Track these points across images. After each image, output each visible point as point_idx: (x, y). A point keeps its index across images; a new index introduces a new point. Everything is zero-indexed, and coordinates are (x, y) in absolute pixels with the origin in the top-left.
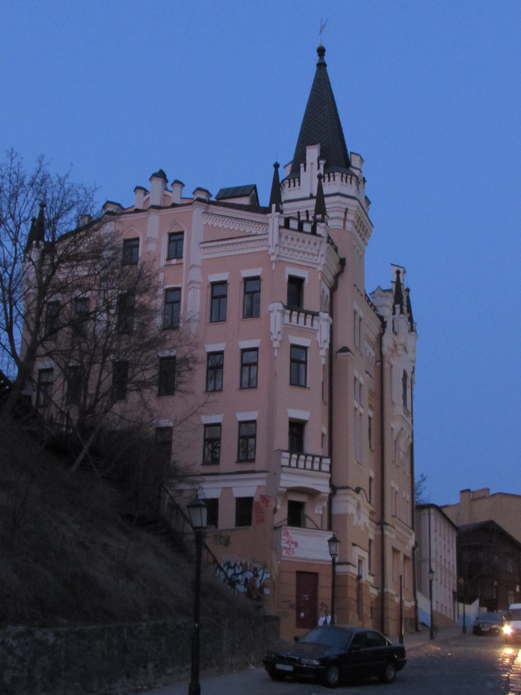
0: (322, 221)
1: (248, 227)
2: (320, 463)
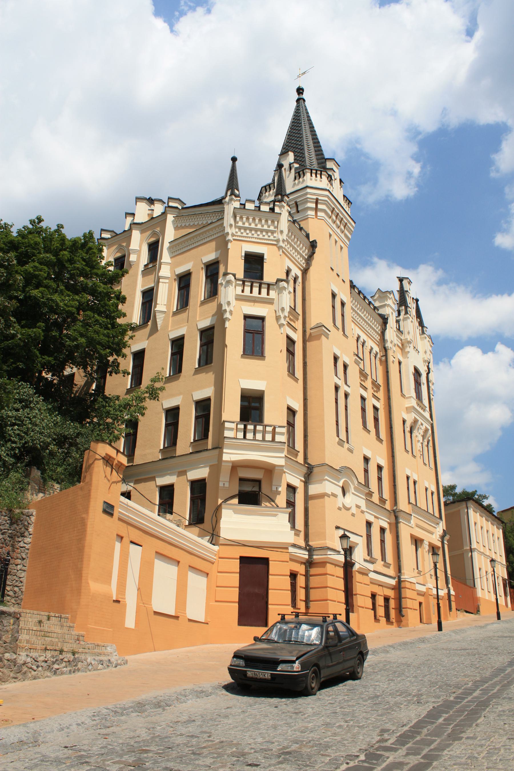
1: (209, 218)
2: (274, 433)
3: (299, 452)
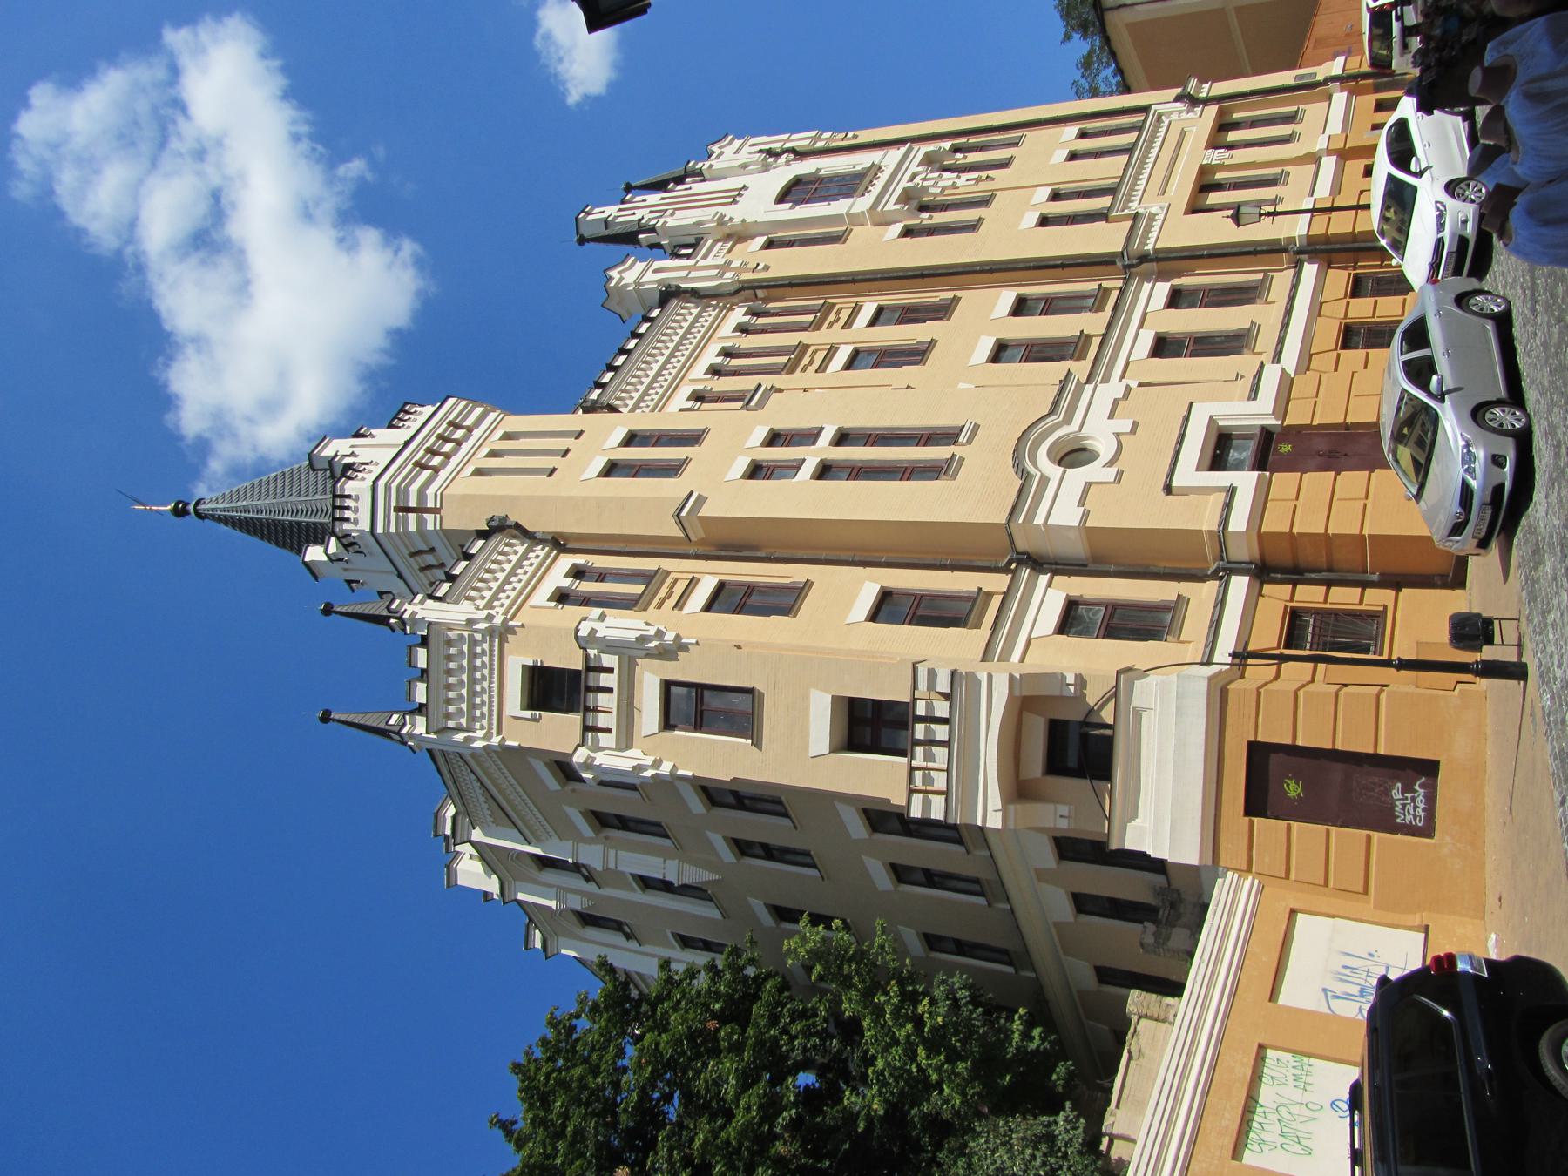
3: (980, 589)
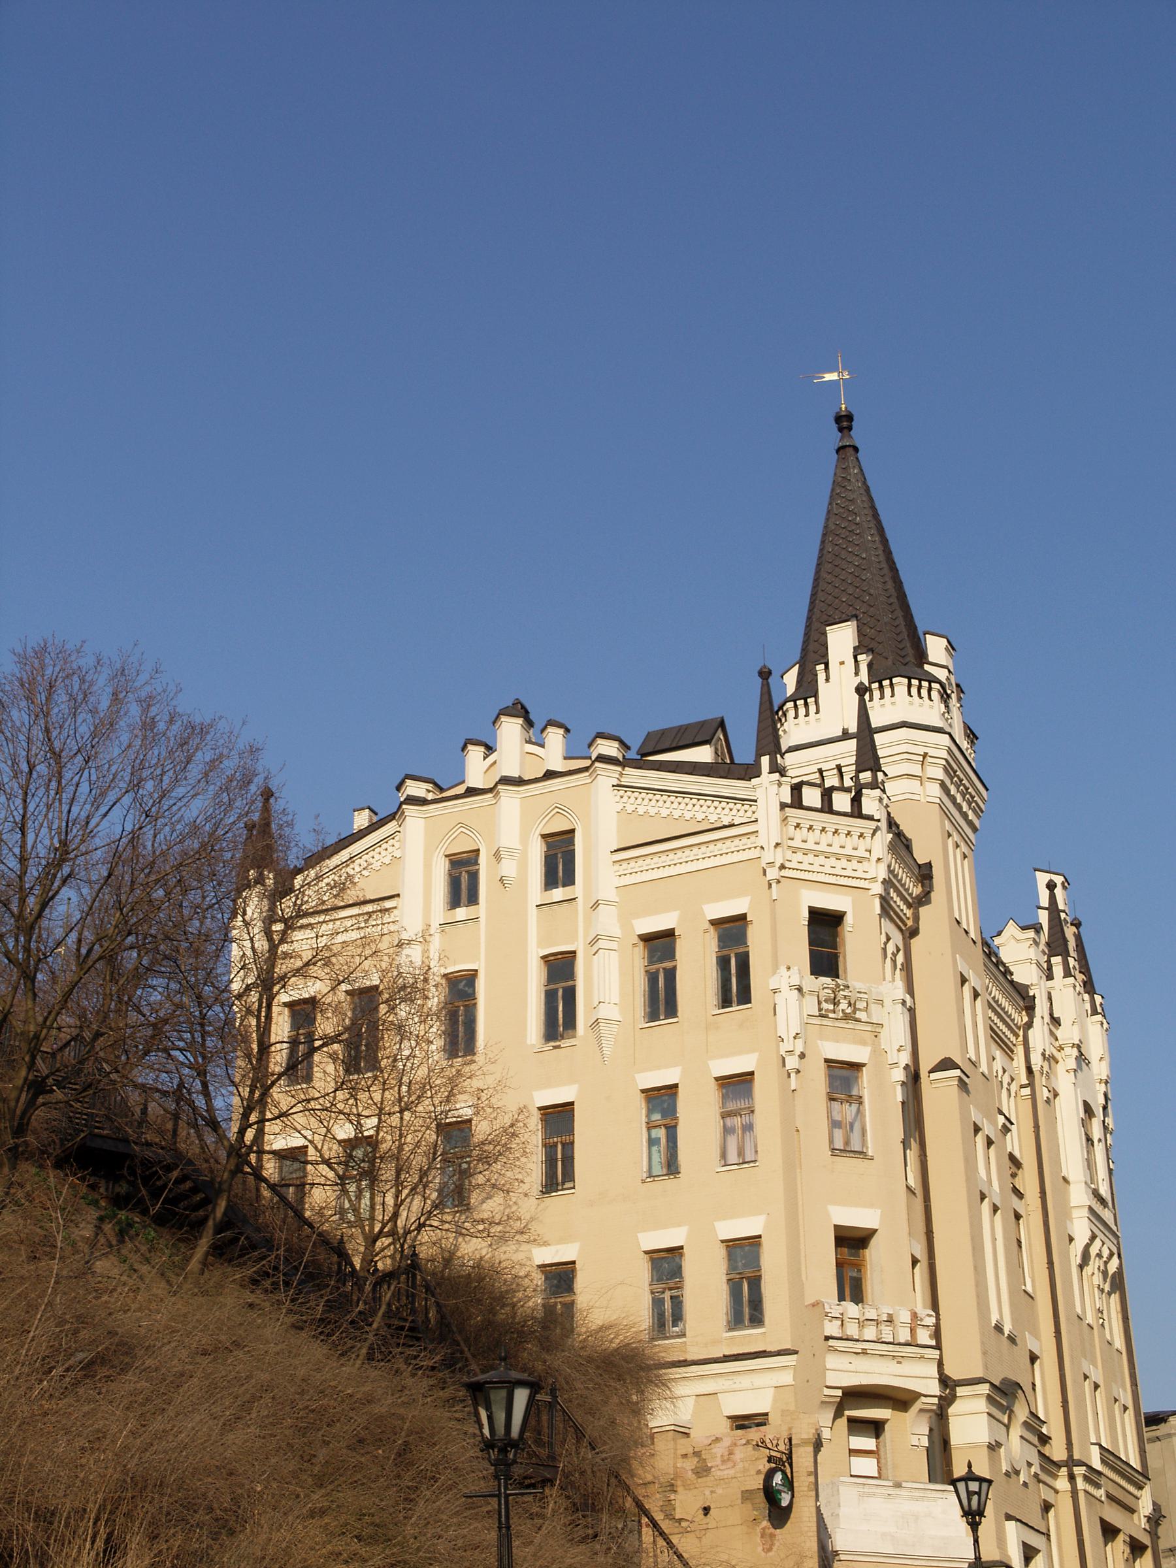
0: (874, 785)
